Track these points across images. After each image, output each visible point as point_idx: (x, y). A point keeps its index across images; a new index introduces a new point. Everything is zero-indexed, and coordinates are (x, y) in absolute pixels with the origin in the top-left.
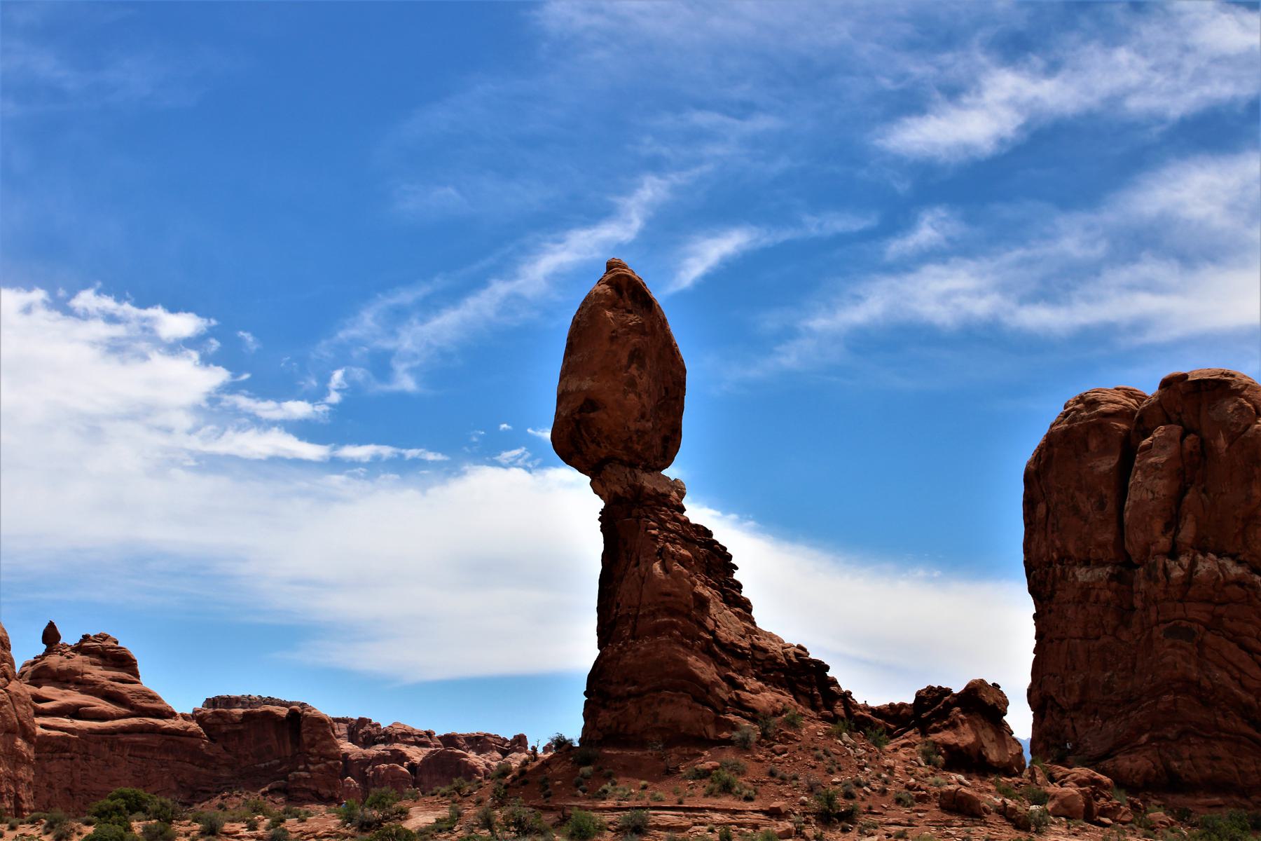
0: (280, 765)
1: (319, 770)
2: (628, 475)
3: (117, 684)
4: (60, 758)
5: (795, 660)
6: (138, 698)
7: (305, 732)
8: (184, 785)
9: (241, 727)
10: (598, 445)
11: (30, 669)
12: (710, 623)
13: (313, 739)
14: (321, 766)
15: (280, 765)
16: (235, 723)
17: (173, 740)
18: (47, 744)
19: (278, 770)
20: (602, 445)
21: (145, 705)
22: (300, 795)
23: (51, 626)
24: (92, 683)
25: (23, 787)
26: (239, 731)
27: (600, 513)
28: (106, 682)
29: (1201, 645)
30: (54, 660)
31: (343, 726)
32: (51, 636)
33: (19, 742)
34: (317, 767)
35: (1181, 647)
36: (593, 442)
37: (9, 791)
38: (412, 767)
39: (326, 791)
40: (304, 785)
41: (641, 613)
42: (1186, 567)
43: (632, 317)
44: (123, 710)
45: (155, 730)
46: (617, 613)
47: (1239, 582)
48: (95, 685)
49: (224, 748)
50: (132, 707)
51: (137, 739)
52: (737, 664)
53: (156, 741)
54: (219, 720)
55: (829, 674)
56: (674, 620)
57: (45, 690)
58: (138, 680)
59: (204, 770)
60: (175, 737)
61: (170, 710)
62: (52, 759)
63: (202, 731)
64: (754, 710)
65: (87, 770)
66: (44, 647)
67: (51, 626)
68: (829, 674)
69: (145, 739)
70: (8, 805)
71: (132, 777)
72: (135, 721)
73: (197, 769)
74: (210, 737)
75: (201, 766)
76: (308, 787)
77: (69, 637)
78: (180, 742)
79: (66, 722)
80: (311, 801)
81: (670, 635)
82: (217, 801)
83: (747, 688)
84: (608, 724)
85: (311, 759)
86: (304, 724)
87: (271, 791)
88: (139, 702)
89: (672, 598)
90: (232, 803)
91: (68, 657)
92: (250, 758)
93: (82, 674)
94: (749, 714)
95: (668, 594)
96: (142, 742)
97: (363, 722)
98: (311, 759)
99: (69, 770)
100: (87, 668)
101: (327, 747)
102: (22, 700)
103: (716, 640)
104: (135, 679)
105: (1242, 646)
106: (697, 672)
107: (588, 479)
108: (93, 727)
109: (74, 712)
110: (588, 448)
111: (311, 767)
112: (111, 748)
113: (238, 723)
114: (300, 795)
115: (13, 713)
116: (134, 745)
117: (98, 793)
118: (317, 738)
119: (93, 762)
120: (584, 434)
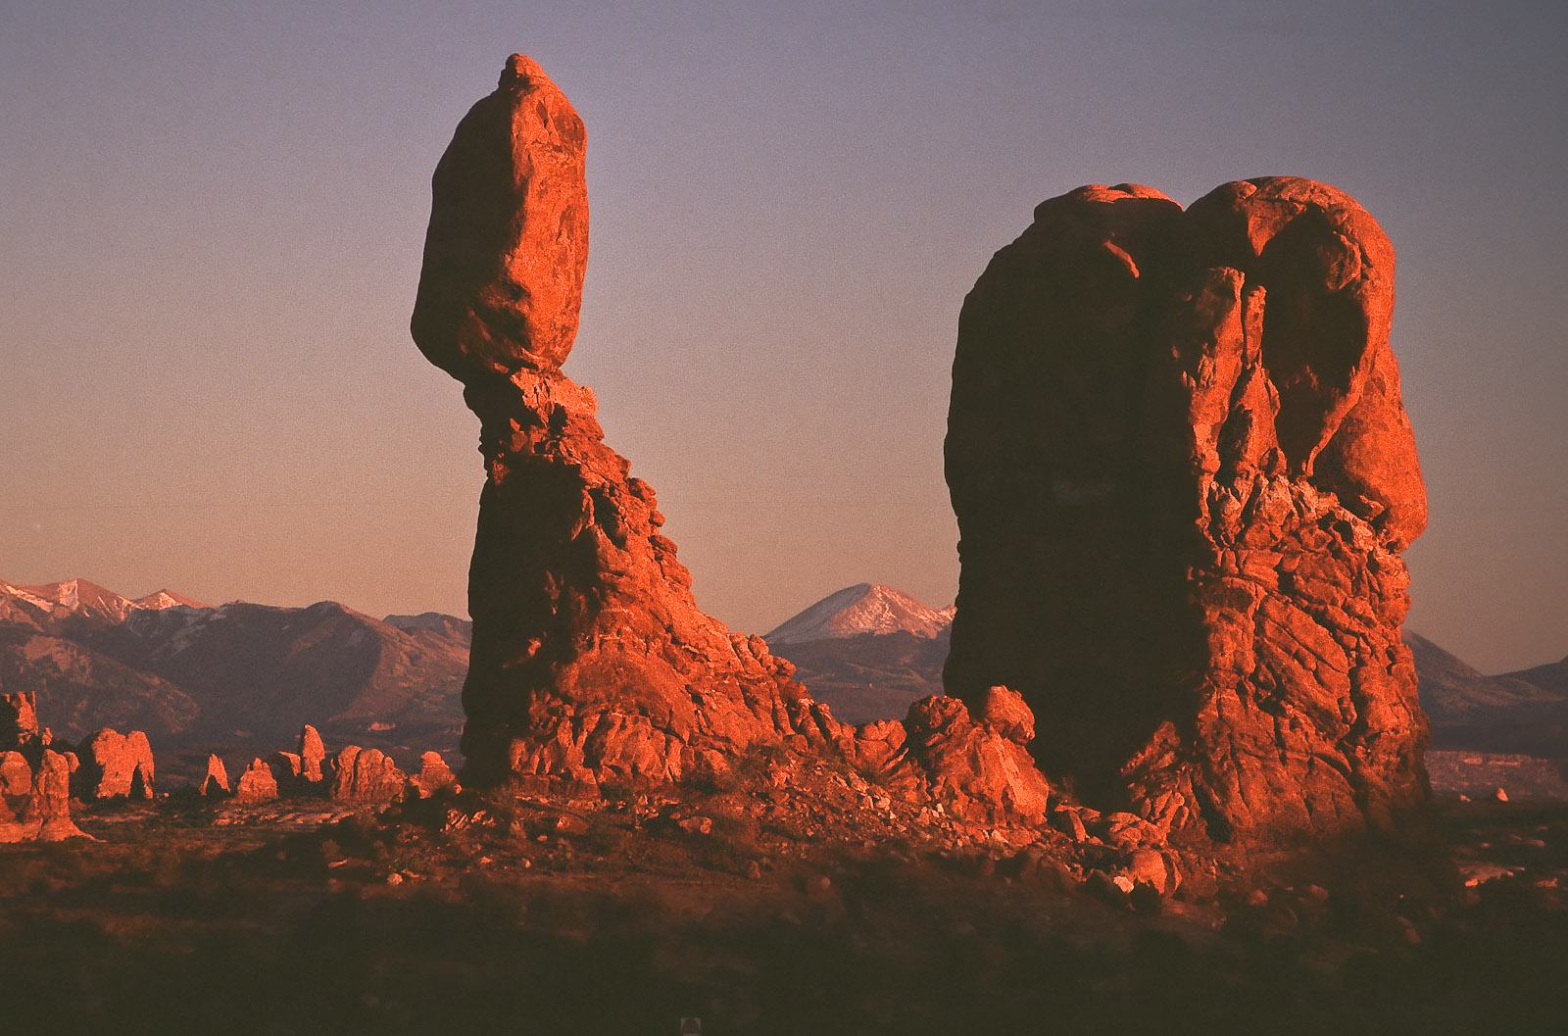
2: (538, 390)
5: (749, 656)
29: (1261, 615)
35: (1230, 620)
42: (1245, 498)
43: (562, 156)
47: (1326, 520)
52: (695, 668)
56: (626, 611)
64: (727, 740)
81: (619, 633)
84: (525, 759)
89: (624, 579)
95: (621, 574)
103: (675, 641)
105: (1321, 618)
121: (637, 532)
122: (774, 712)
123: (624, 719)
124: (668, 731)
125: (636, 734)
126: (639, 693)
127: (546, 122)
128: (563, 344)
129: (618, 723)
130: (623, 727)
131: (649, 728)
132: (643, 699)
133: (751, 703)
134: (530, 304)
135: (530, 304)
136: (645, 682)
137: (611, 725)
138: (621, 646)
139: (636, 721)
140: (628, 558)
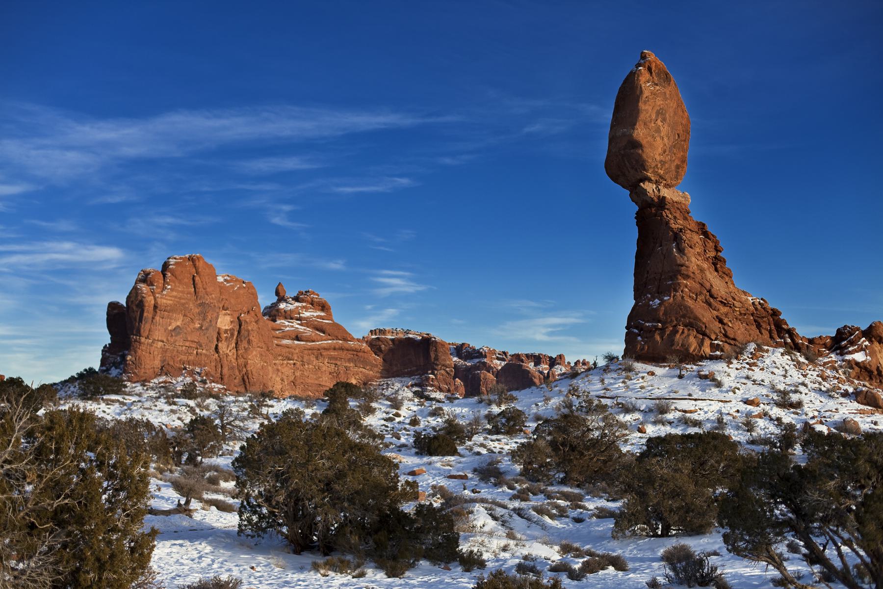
2: (655, 190)
10: (636, 170)
12: (708, 285)
20: (638, 170)
27: (636, 214)
36: (632, 168)
41: (663, 277)
43: (658, 88)
46: (647, 277)
52: (724, 310)
55: (781, 317)
64: (734, 339)
68: (781, 317)
81: (682, 291)
83: (730, 325)
94: (732, 342)
95: (682, 266)
103: (712, 296)
106: (701, 317)
107: (627, 192)
110: (629, 172)
120: (626, 162)
121: (691, 247)
122: (770, 332)
123: (683, 329)
124: (704, 334)
125: (689, 335)
126: (689, 318)
127: (651, 73)
128: (663, 169)
129: (681, 331)
130: (683, 332)
131: (695, 333)
132: (691, 320)
133: (759, 326)
134: (642, 150)
135: (642, 150)
136: (692, 313)
137: (677, 332)
138: (683, 297)
139: (689, 330)
140: (686, 258)
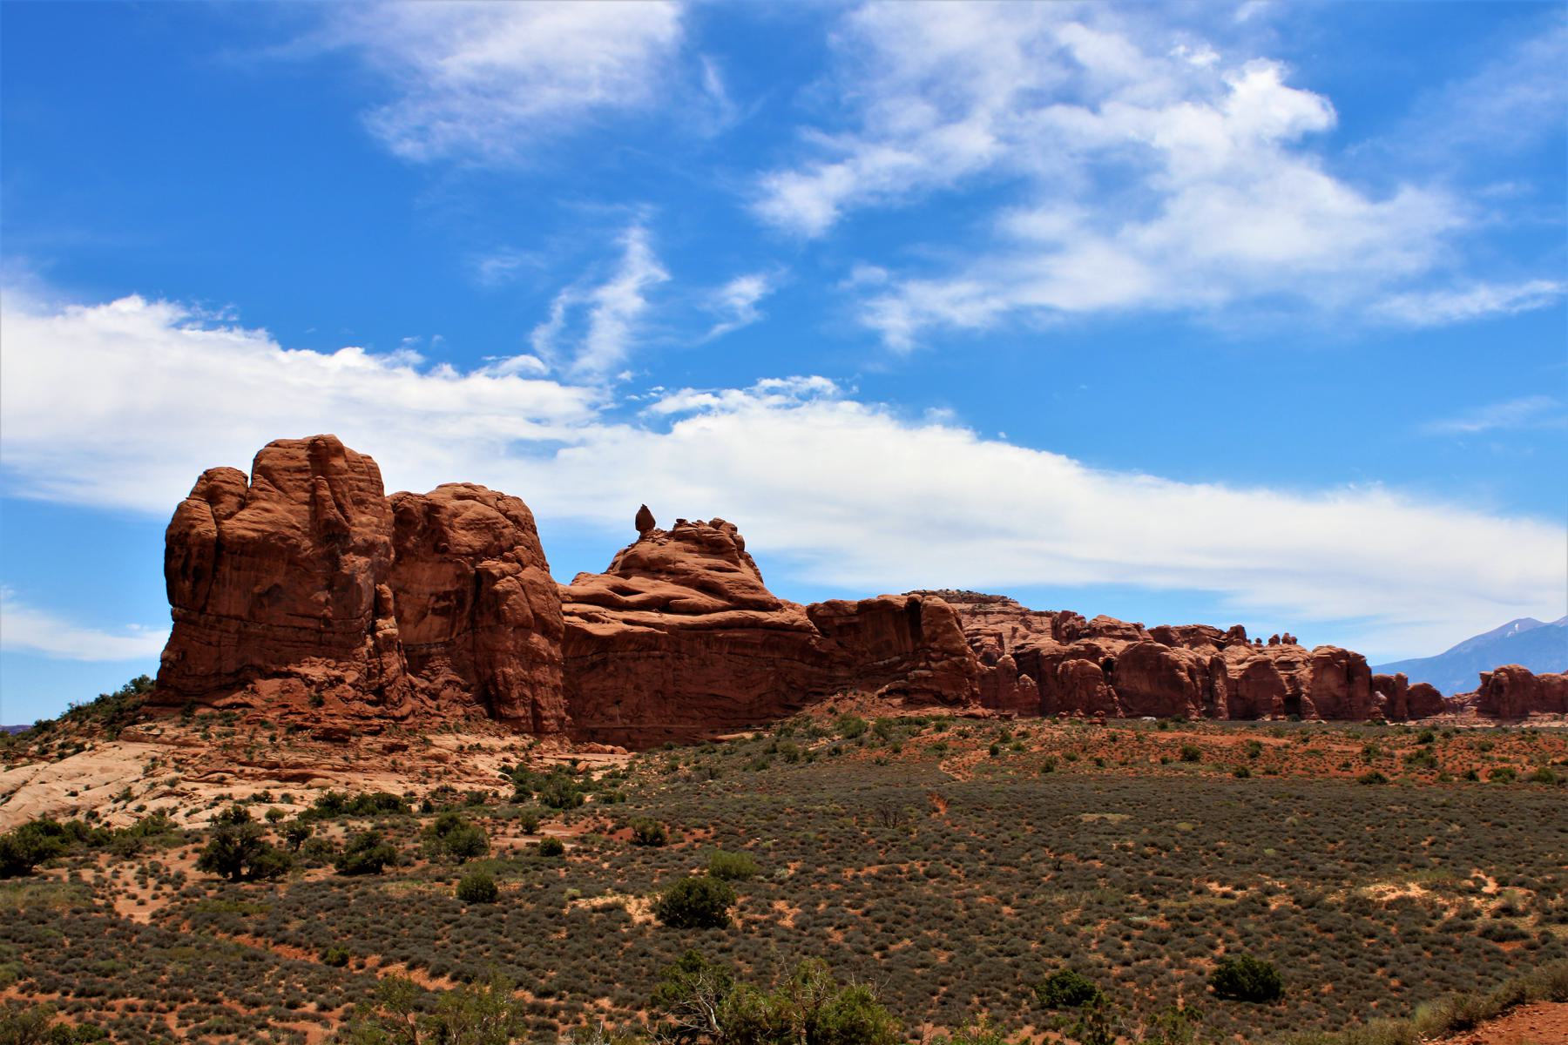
0: (901, 662)
1: (942, 668)
3: (713, 573)
4: (649, 657)
6: (737, 588)
7: (925, 625)
8: (794, 686)
9: (856, 619)
11: (622, 558)
13: (934, 632)
14: (944, 663)
15: (901, 662)
16: (850, 615)
17: (779, 636)
18: (630, 642)
19: (899, 669)
21: (745, 596)
22: (920, 697)
23: (644, 510)
24: (685, 572)
25: (541, 691)
26: (855, 624)
28: (701, 571)
30: (648, 550)
31: (1046, 620)
32: (644, 520)
33: (536, 638)
34: (940, 664)
37: (522, 696)
38: (1108, 665)
39: (950, 692)
40: (925, 686)
44: (720, 602)
45: (756, 624)
48: (689, 574)
49: (840, 644)
50: (730, 599)
51: (736, 635)
53: (758, 636)
54: (831, 612)
57: (635, 582)
58: (738, 568)
59: (816, 669)
60: (780, 632)
61: (774, 601)
62: (639, 658)
63: (812, 625)
65: (681, 670)
66: (639, 533)
67: (644, 510)
69: (744, 634)
70: (521, 712)
71: (733, 678)
72: (733, 614)
73: (808, 668)
74: (822, 632)
75: (812, 665)
76: (929, 687)
77: (665, 523)
78: (787, 638)
79: (654, 616)
80: (934, 704)
82: (829, 704)
85: (933, 655)
86: (923, 615)
87: (890, 693)
88: (738, 593)
90: (844, 707)
91: (660, 544)
92: (868, 655)
93: (675, 563)
96: (742, 637)
97: (1066, 615)
98: (933, 655)
99: (659, 670)
100: (680, 556)
101: (951, 641)
102: (539, 589)
104: (735, 567)
108: (684, 622)
109: (664, 605)
111: (933, 665)
112: (708, 645)
113: (853, 615)
114: (920, 697)
115: (526, 605)
116: (734, 642)
117: (693, 696)
118: (939, 631)
119: (687, 661)
